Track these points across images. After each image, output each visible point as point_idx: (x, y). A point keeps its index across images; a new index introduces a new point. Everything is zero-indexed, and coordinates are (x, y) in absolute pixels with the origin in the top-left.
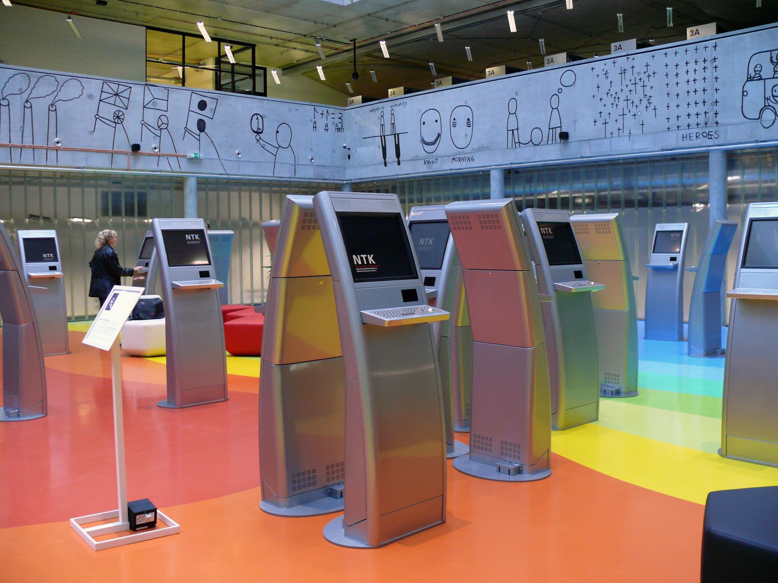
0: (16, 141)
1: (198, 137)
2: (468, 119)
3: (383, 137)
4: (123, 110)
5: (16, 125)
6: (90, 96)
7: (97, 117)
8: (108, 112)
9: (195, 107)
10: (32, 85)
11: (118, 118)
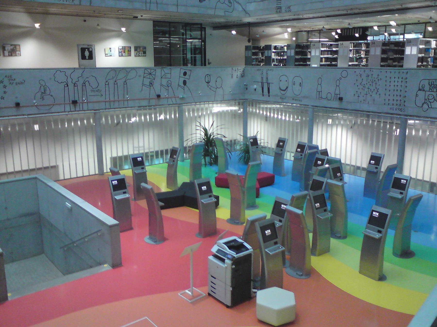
0: (112, 99)
1: (183, 88)
2: (300, 83)
3: (262, 83)
4: (153, 80)
5: (112, 91)
6: (140, 76)
7: (143, 84)
8: (147, 82)
9: (182, 75)
11: (151, 84)
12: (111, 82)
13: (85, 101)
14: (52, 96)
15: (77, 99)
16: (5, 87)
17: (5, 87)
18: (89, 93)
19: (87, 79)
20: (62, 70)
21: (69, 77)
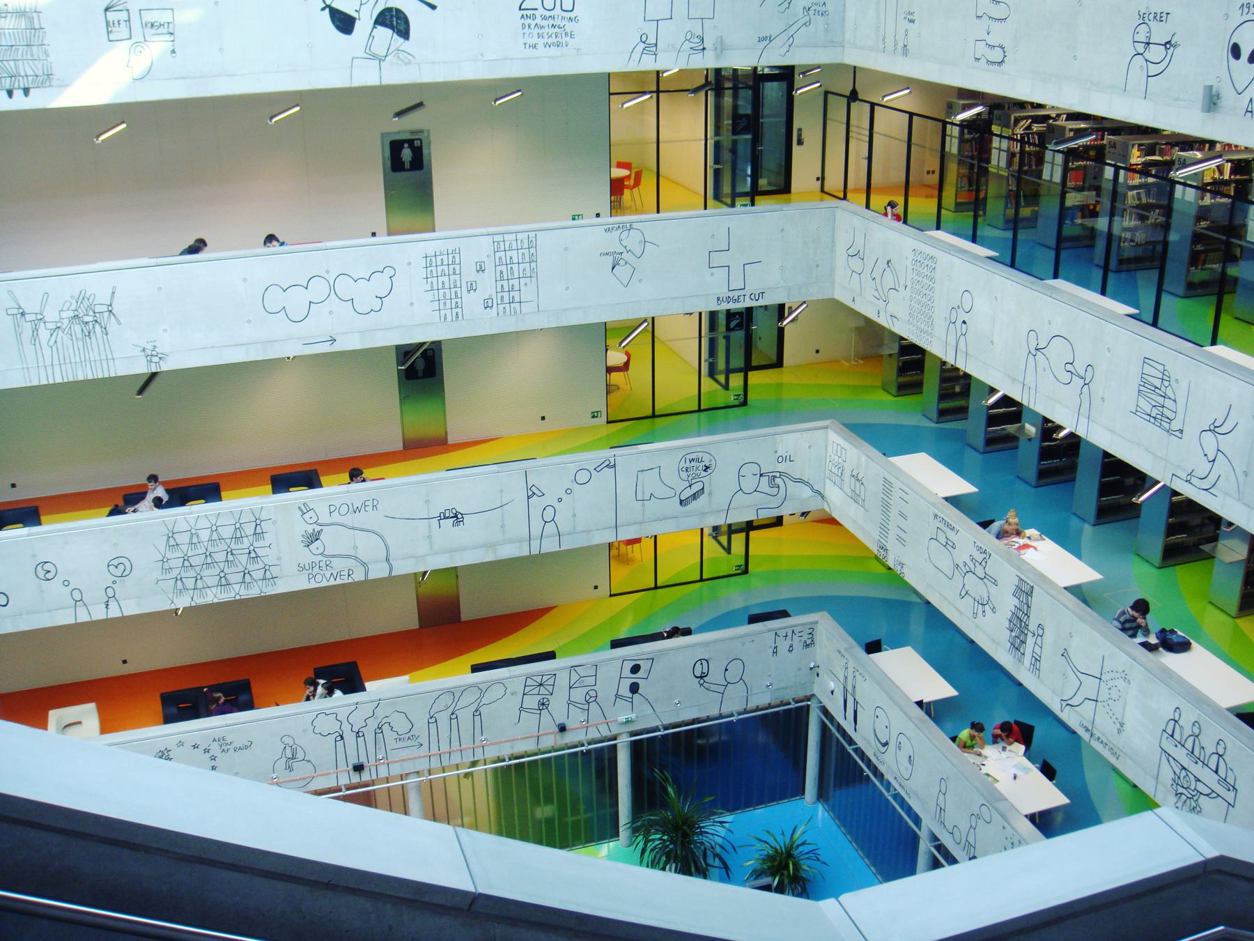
1: (630, 700)
2: (910, 757)
5: (444, 734)
7: (522, 709)
8: (531, 702)
10: (456, 700)
11: (543, 705)
12: (443, 719)
13: (382, 761)
14: (309, 761)
15: (363, 760)
16: (213, 758)
17: (213, 758)
18: (391, 743)
19: (386, 720)
20: (328, 712)
21: (345, 722)
